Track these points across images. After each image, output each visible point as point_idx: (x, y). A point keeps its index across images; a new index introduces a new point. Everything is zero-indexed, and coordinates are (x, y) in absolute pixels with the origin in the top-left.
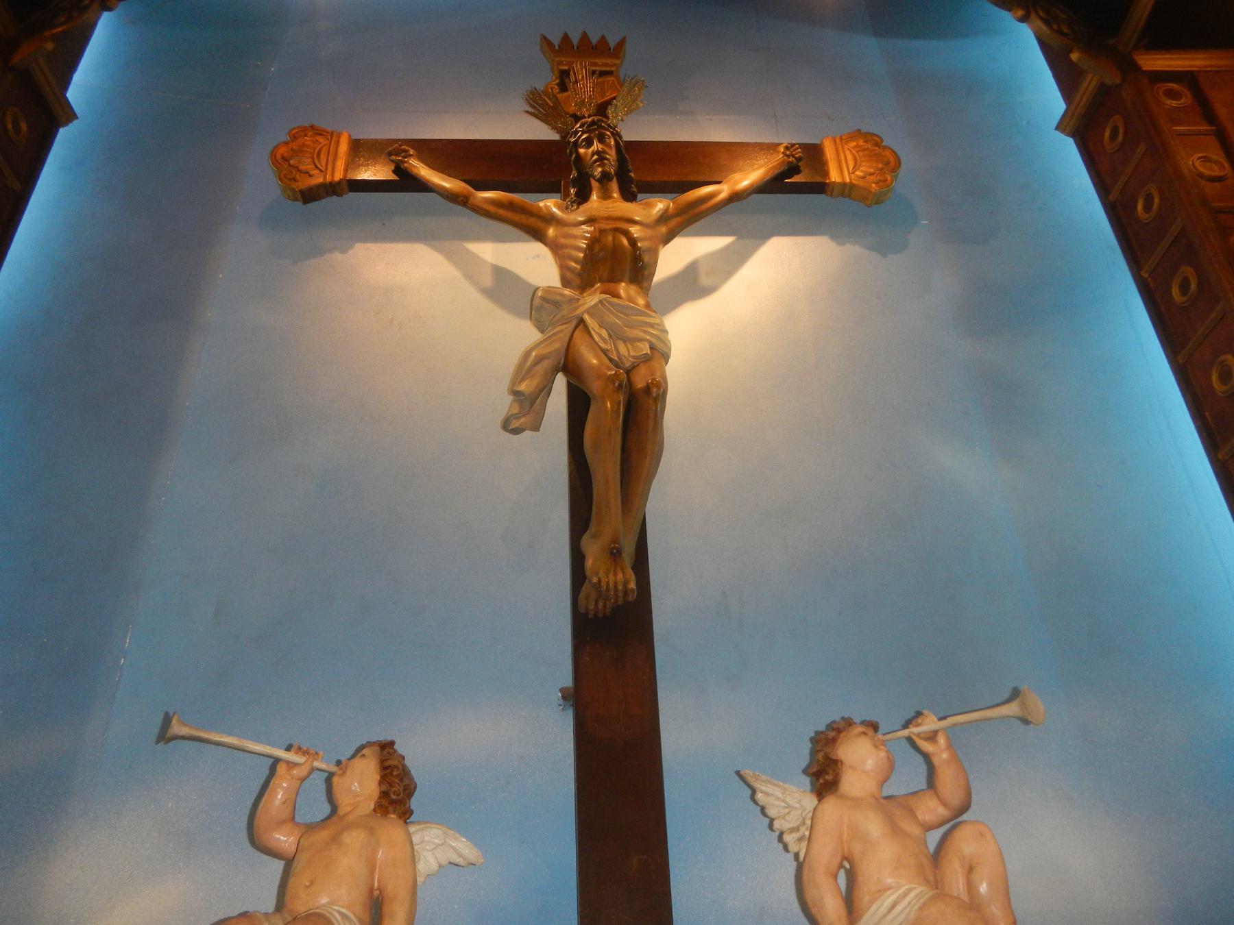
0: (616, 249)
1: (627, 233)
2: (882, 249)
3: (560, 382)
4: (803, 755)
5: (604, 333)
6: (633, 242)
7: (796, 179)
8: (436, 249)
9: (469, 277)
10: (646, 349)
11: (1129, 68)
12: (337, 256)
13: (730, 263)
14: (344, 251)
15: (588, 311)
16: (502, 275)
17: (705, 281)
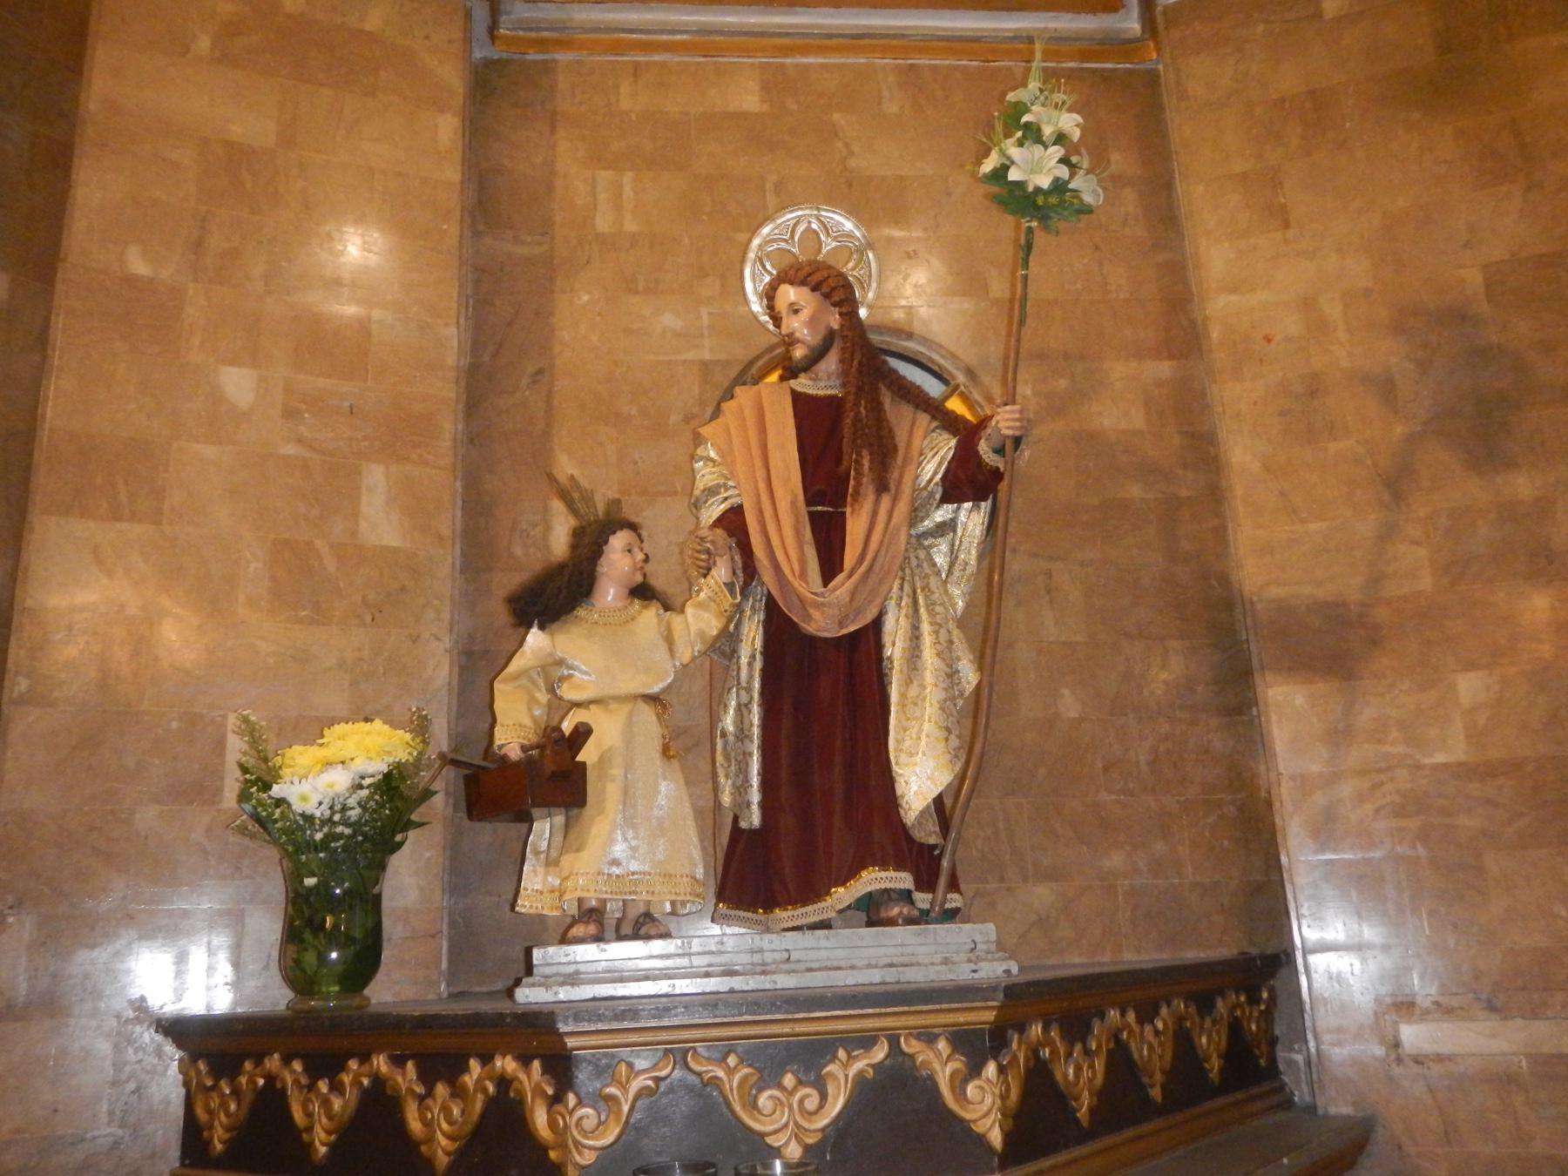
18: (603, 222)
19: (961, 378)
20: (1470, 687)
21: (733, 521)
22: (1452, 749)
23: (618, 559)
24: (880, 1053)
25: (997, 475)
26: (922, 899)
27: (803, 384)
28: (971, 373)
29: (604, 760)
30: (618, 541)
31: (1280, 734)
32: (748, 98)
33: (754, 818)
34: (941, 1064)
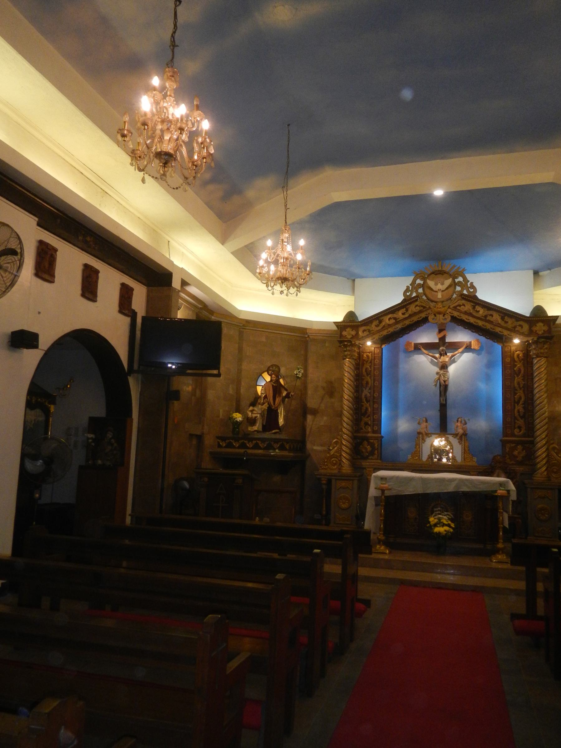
0: (445, 366)
1: (445, 364)
2: (478, 354)
3: (439, 381)
4: (456, 419)
5: (443, 377)
6: (446, 365)
7: (468, 347)
8: (424, 356)
9: (428, 361)
10: (447, 379)
11: (503, 345)
12: (413, 357)
13: (460, 356)
14: (413, 356)
15: (442, 374)
16: (431, 359)
17: (456, 360)
18: (248, 354)
19: (282, 377)
20: (325, 418)
21: (266, 397)
22: (322, 424)
23: (259, 401)
24: (281, 443)
25: (290, 397)
26: (280, 433)
27: (273, 384)
28: (284, 377)
29: (258, 419)
30: (259, 399)
31: (308, 420)
32: (264, 340)
33: (265, 424)
34: (285, 444)
